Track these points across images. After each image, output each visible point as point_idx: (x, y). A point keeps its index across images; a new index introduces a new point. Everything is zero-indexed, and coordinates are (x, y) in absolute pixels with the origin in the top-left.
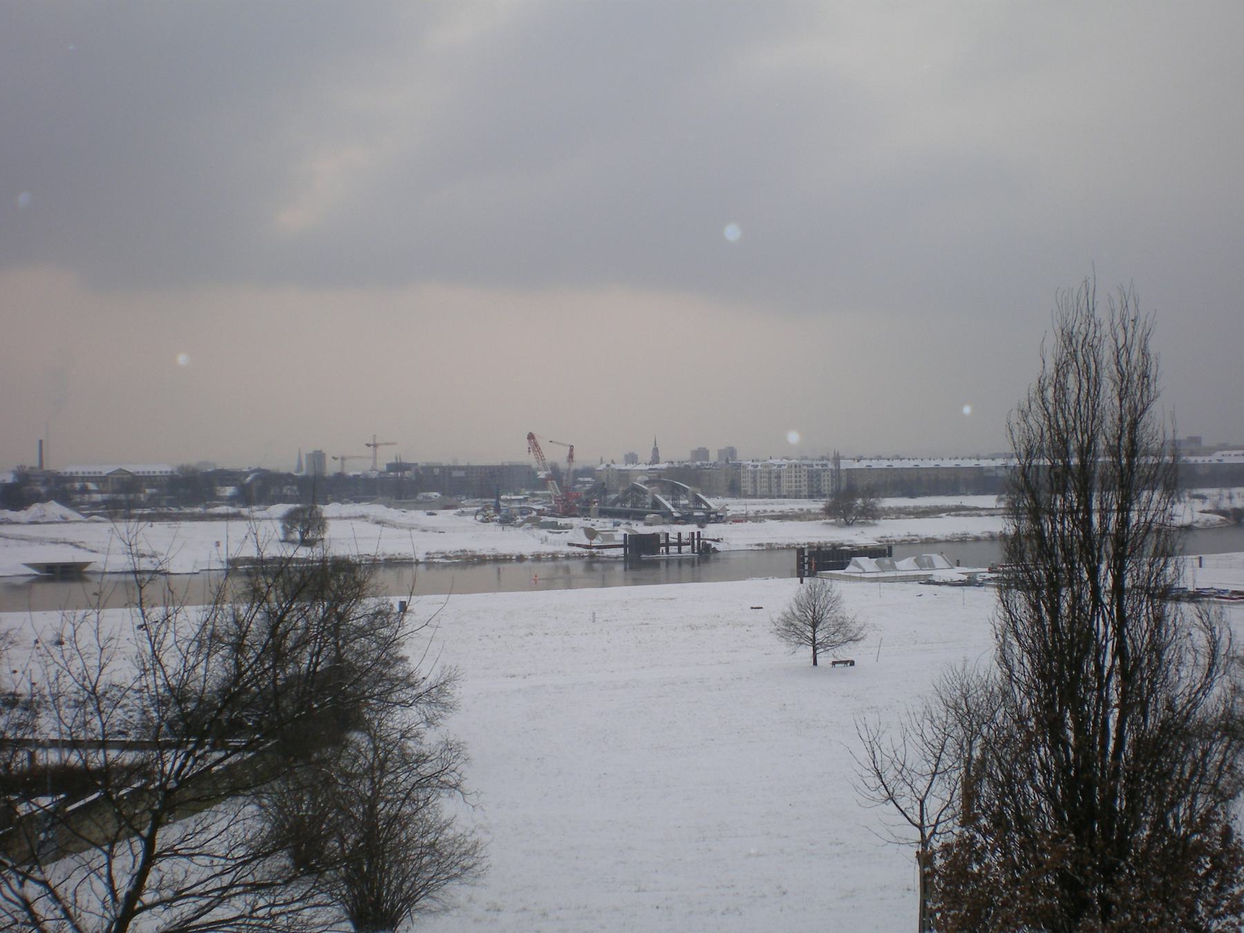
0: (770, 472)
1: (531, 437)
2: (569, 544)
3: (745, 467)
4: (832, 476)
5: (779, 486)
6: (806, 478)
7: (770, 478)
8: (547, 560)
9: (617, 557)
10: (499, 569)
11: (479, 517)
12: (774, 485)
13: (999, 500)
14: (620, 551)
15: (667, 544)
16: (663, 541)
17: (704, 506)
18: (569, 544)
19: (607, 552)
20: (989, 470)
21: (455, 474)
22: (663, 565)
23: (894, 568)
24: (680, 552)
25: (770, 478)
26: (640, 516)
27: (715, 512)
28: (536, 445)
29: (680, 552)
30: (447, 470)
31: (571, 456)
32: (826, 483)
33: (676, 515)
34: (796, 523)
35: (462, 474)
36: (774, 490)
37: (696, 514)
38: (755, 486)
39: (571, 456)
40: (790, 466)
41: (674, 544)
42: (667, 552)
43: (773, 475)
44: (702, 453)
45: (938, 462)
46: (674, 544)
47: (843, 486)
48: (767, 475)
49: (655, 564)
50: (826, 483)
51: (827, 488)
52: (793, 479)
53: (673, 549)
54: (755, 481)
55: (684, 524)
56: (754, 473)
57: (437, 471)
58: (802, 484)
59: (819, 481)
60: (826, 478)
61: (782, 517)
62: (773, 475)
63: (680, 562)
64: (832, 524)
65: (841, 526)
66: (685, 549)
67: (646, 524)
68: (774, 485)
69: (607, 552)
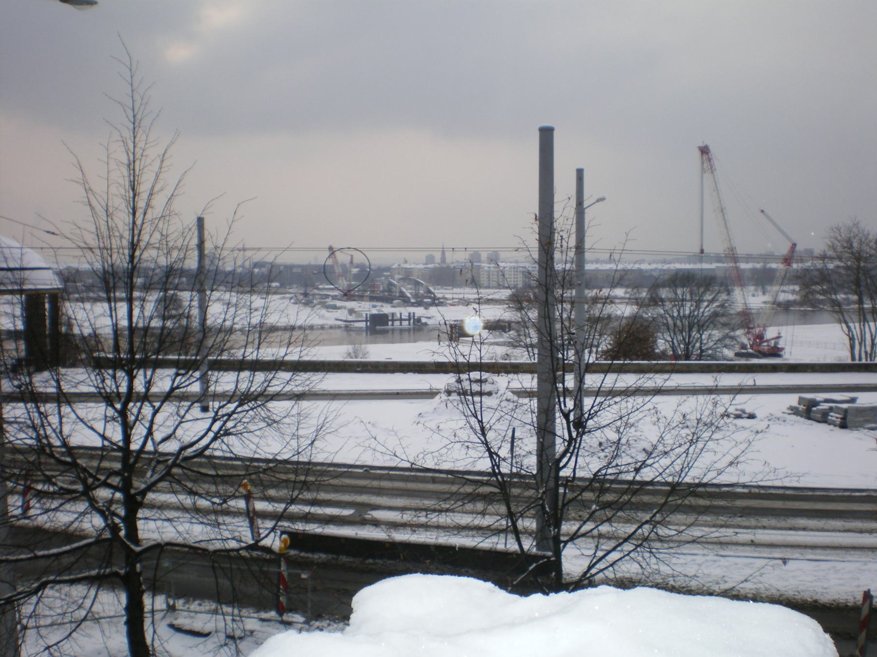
2: (337, 320)
8: (318, 329)
9: (362, 328)
11: (292, 301)
14: (363, 325)
15: (393, 320)
16: (390, 318)
18: (337, 320)
19: (357, 325)
20: (647, 271)
21: (295, 270)
22: (390, 332)
24: (401, 325)
25: (498, 275)
26: (388, 300)
27: (439, 299)
29: (401, 325)
35: (299, 270)
40: (510, 268)
41: (405, 320)
42: (393, 325)
46: (405, 320)
49: (385, 332)
53: (397, 323)
54: (489, 278)
55: (417, 307)
56: (489, 272)
57: (282, 268)
63: (402, 331)
66: (405, 323)
67: (392, 307)
69: (357, 325)
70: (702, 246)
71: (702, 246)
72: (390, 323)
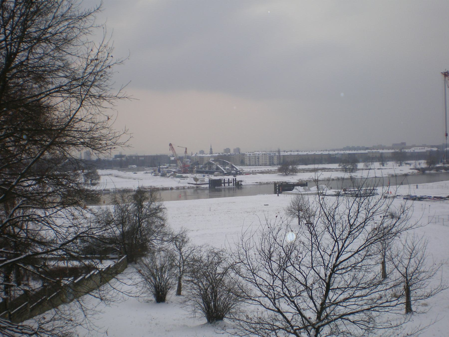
0: (255, 157)
1: (170, 145)
2: (189, 183)
3: (246, 155)
4: (278, 158)
5: (259, 161)
6: (268, 159)
7: (255, 159)
8: (181, 189)
9: (207, 188)
10: (417, 185)
11: (153, 174)
12: (257, 161)
13: (339, 166)
14: (208, 186)
15: (224, 183)
16: (223, 182)
17: (235, 169)
18: (189, 183)
19: (203, 186)
20: (333, 155)
21: (141, 159)
22: (223, 190)
23: (309, 190)
24: (229, 185)
25: (255, 159)
26: (212, 173)
27: (239, 171)
28: (172, 148)
29: (229, 185)
30: (138, 157)
31: (186, 152)
32: (275, 160)
33: (225, 172)
34: (268, 175)
35: (143, 158)
36: (257, 163)
37: (232, 172)
38: (250, 162)
39: (186, 152)
40: (263, 154)
41: (227, 183)
42: (224, 186)
43: (257, 157)
44: (227, 150)
45: (307, 152)
46: (227, 183)
47: (282, 161)
48: (254, 158)
49: (220, 190)
50: (275, 160)
51: (275, 162)
52: (264, 159)
53: (227, 185)
54: (250, 160)
56: (249, 157)
57: (134, 158)
58: (267, 161)
59: (273, 159)
60: (275, 158)
61: (262, 173)
62: (257, 157)
63: (229, 189)
64: (281, 175)
65: (284, 176)
66: (230, 184)
67: (215, 176)
68: (257, 161)
69: (203, 186)
70: (446, 132)
71: (446, 132)
72: (223, 185)
